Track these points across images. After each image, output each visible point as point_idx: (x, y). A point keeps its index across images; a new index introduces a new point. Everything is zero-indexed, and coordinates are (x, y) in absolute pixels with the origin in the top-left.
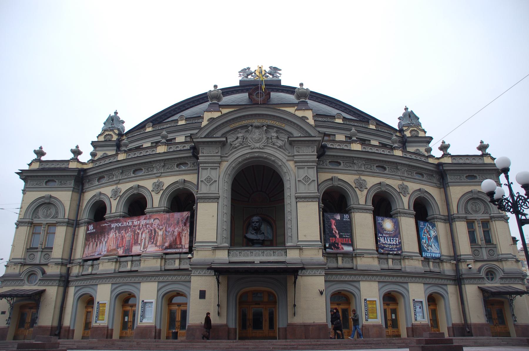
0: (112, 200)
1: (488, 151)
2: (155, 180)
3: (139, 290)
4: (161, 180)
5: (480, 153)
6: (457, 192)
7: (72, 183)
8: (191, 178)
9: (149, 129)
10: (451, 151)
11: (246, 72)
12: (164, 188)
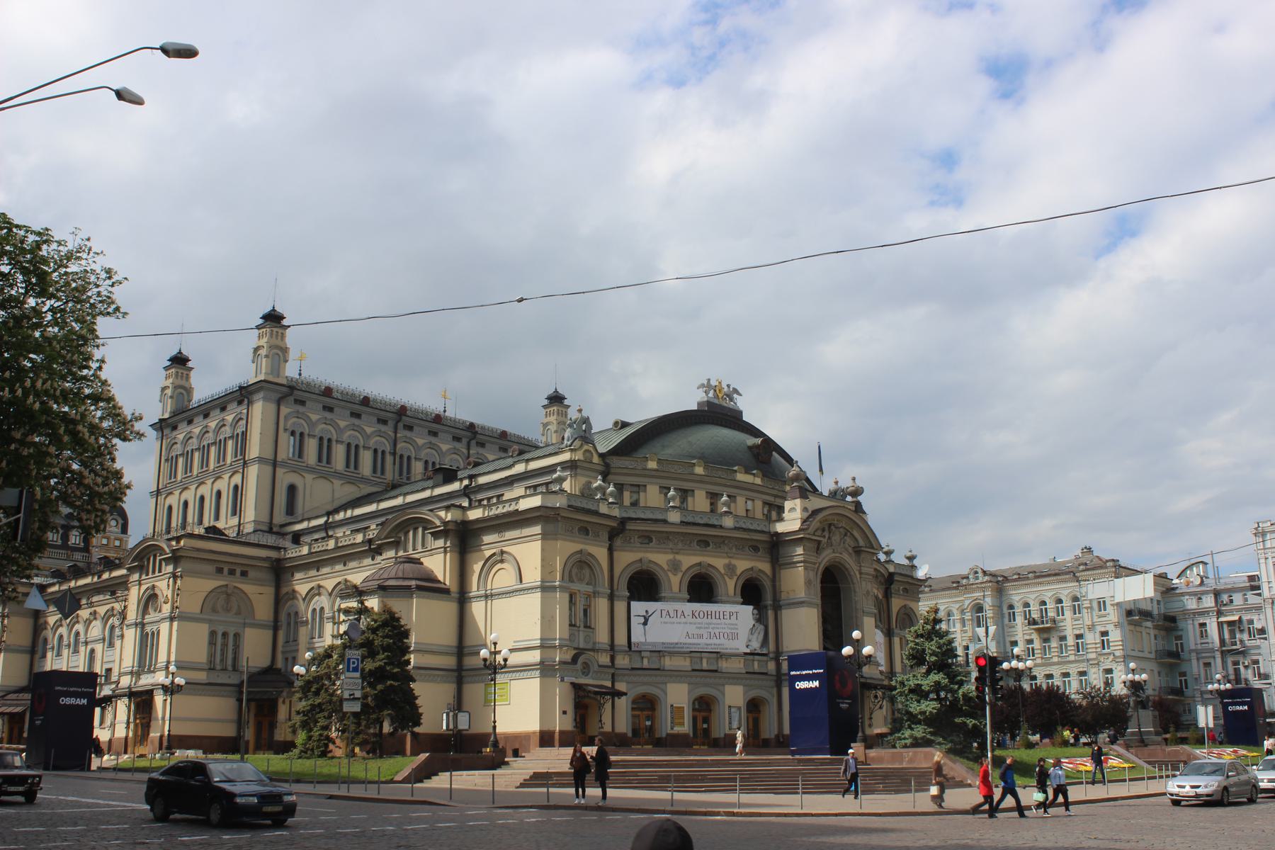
0: (670, 575)
1: (915, 562)
2: (726, 561)
3: (724, 694)
4: (734, 562)
5: (906, 562)
6: (896, 604)
7: (606, 536)
8: (765, 567)
9: (652, 465)
10: (893, 557)
11: (707, 386)
12: (738, 572)
